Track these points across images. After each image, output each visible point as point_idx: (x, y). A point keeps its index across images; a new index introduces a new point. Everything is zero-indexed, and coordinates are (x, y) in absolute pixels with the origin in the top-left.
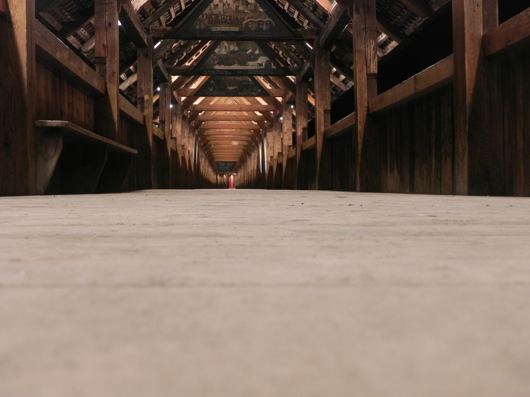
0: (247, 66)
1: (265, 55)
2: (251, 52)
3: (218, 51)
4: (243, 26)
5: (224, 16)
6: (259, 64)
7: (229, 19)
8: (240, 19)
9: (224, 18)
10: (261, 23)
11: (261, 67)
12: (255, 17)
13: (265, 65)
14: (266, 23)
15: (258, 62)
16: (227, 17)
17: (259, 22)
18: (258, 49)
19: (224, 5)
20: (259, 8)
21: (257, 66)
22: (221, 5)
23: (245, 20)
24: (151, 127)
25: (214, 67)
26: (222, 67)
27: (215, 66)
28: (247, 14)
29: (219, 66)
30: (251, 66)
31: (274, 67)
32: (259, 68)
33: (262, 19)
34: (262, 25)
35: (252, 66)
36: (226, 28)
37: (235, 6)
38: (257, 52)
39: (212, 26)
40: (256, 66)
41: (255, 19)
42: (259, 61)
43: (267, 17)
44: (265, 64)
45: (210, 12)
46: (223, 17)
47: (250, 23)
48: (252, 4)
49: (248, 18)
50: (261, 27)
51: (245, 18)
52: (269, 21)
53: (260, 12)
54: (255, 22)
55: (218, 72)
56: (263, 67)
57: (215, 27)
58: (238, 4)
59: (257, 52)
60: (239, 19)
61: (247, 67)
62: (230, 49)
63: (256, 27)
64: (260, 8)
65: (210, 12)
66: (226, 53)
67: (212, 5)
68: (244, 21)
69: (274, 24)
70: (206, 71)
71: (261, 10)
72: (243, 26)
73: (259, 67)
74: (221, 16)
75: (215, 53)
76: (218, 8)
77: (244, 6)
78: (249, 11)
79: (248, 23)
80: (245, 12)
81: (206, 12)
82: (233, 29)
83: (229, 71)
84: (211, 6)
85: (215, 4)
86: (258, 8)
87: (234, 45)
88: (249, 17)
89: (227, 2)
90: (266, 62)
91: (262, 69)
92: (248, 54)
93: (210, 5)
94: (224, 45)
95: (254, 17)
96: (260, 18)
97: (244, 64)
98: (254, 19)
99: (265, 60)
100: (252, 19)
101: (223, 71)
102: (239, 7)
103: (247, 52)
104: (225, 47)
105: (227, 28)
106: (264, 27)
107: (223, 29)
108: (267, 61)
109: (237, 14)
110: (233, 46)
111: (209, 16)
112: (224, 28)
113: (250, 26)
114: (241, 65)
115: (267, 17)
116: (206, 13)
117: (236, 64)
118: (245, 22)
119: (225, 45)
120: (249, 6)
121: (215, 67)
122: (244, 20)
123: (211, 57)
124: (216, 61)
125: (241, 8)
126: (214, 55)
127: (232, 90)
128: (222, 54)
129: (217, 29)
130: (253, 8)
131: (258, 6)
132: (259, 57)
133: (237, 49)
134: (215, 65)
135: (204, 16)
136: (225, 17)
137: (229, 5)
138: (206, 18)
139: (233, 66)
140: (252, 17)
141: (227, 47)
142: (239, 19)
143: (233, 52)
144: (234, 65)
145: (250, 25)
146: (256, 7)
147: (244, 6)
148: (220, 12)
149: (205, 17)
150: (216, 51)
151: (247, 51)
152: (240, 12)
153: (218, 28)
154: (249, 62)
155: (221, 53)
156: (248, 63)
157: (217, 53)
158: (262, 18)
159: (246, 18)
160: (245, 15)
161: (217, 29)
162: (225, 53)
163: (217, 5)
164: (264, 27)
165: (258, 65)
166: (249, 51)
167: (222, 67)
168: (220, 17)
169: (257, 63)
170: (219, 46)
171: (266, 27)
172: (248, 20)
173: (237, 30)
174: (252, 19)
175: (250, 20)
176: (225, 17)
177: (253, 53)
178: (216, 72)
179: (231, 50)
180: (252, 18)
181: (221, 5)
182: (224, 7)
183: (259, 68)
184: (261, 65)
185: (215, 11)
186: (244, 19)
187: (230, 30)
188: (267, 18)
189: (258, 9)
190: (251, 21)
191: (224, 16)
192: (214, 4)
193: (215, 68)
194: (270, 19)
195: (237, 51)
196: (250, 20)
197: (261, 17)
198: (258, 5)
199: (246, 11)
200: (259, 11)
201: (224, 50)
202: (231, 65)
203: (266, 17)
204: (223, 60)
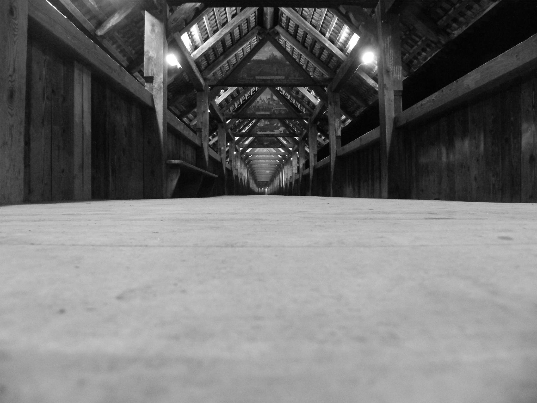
0: (274, 132)
1: (283, 126)
3: (259, 125)
10: (281, 110)
11: (281, 133)
14: (284, 110)
17: (280, 109)
19: (262, 101)
22: (260, 101)
24: (71, 213)
26: (261, 133)
31: (288, 132)
37: (268, 102)
38: (279, 125)
41: (278, 108)
42: (280, 130)
47: (276, 110)
49: (275, 108)
50: (281, 112)
53: (281, 105)
54: (278, 110)
58: (269, 101)
59: (279, 125)
67: (256, 101)
69: (288, 110)
71: (281, 104)
79: (274, 111)
83: (265, 134)
87: (267, 121)
90: (284, 130)
97: (272, 131)
100: (277, 108)
104: (263, 123)
111: (254, 107)
118: (273, 110)
120: (275, 102)
122: (272, 108)
125: (271, 103)
127: (267, 144)
130: (277, 103)
134: (257, 132)
137: (265, 101)
143: (267, 125)
144: (267, 131)
146: (278, 102)
148: (260, 105)
149: (252, 107)
150: (258, 124)
152: (270, 104)
157: (259, 125)
159: (273, 108)
162: (263, 125)
163: (259, 101)
166: (276, 124)
167: (261, 133)
168: (260, 107)
172: (275, 109)
174: (277, 108)
177: (277, 125)
180: (277, 107)
181: (260, 101)
183: (280, 133)
184: (281, 131)
185: (258, 105)
190: (276, 109)
194: (286, 108)
195: (269, 125)
198: (280, 101)
199: (273, 104)
201: (262, 124)
202: (266, 131)
204: (262, 129)
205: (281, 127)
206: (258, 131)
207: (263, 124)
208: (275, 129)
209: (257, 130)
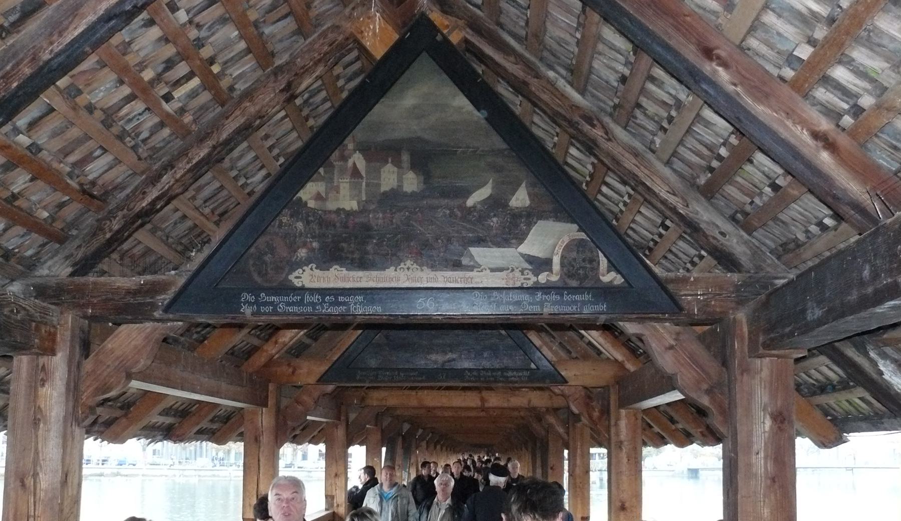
0: (470, 268)
1: (562, 213)
2: (484, 202)
3: (318, 197)
6: (530, 259)
11: (543, 278)
13: (562, 265)
15: (524, 248)
18: (524, 185)
21: (522, 272)
25: (291, 277)
27: (296, 274)
29: (317, 272)
30: (488, 271)
32: (530, 283)
35: (492, 270)
38: (520, 199)
40: (517, 274)
44: (563, 257)
55: (313, 305)
56: (554, 278)
59: (520, 199)
61: (469, 274)
62: (379, 185)
66: (358, 203)
70: (252, 299)
73: (530, 275)
75: (302, 204)
87: (398, 164)
90: (567, 248)
91: (547, 289)
92: (474, 207)
94: (350, 163)
99: (566, 240)
101: (341, 299)
103: (468, 198)
104: (356, 173)
108: (576, 245)
110: (396, 169)
114: (433, 267)
117: (409, 263)
119: (354, 164)
121: (297, 277)
123: (280, 225)
124: (304, 245)
126: (292, 216)
128: (339, 211)
132: (530, 225)
133: (415, 181)
134: (300, 264)
139: (390, 272)
141: (363, 174)
143: (391, 199)
150: (308, 193)
151: (467, 193)
154: (474, 250)
155: (331, 206)
156: (472, 257)
157: (312, 204)
162: (352, 205)
165: (527, 266)
169: (523, 255)
170: (321, 170)
177: (497, 203)
178: (301, 303)
179: (384, 188)
184: (540, 264)
193: (298, 283)
201: (345, 185)
205: (542, 216)
206: (308, 262)
207: (355, 187)
208: (480, 241)
209: (293, 248)
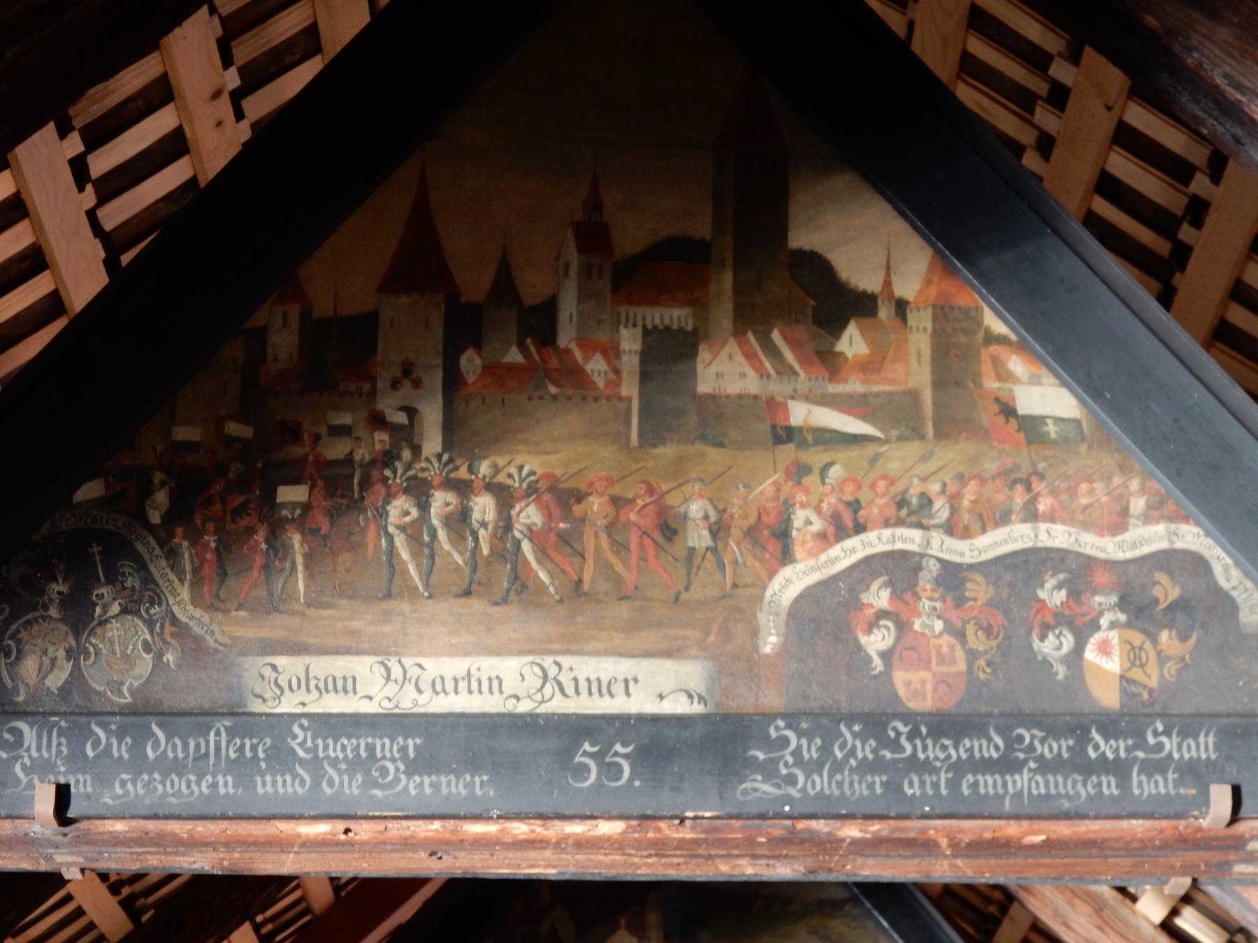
4: (770, 642)
5: (463, 489)
7: (531, 532)
8: (718, 530)
9: (460, 521)
10: (1053, 595)
12: (954, 501)
16: (504, 496)
20: (1004, 375)
23: (799, 552)
28: (816, 458)
33: (1057, 536)
34: (1052, 622)
36: (488, 665)
39: (270, 648)
43: (1138, 504)
45: (235, 429)
46: (441, 501)
47: (878, 597)
48: (901, 307)
50: (1053, 646)
51: (799, 517)
52: (1168, 560)
53: (1031, 427)
54: (952, 576)
57: (322, 666)
60: (698, 537)
63: (972, 655)
64: (1017, 365)
65: (235, 429)
68: (786, 557)
72: (770, 642)
74: (419, 490)
76: (373, 379)
77: (776, 335)
78: (863, 417)
80: (786, 435)
81: (183, 433)
82: (604, 688)
84: (262, 334)
85: (323, 308)
86: (987, 369)
88: (855, 506)
89: (505, 284)
93: (258, 319)
95: (941, 510)
96: (1032, 516)
98: (937, 538)
100: (909, 539)
102: (704, 354)
105: (510, 668)
106: (1104, 648)
107: (437, 687)
109: (667, 451)
112: (454, 666)
113: (876, 642)
115: (1138, 504)
116: (192, 446)
129: (347, 686)
131: (1001, 340)
135: (146, 492)
136: (484, 507)
138: (170, 519)
140: (901, 503)
142: (698, 537)
145: (871, 627)
147: (776, 335)
153: (363, 667)
158: (1051, 518)
159: (806, 522)
160: (799, 472)
161: (347, 686)
164: (1090, 654)
168: (400, 509)
171: (1134, 657)
173: (678, 706)
174: (909, 539)
175: (876, 541)
176: (484, 507)
182: (470, 362)
186: (783, 535)
187: (558, 705)
188: (1147, 519)
189: (991, 384)
191: (463, 489)
192: (305, 315)
196: (876, 541)
197: (1043, 505)
198: (995, 324)
199: (800, 414)
200: (1008, 411)
203: (1125, 512)
